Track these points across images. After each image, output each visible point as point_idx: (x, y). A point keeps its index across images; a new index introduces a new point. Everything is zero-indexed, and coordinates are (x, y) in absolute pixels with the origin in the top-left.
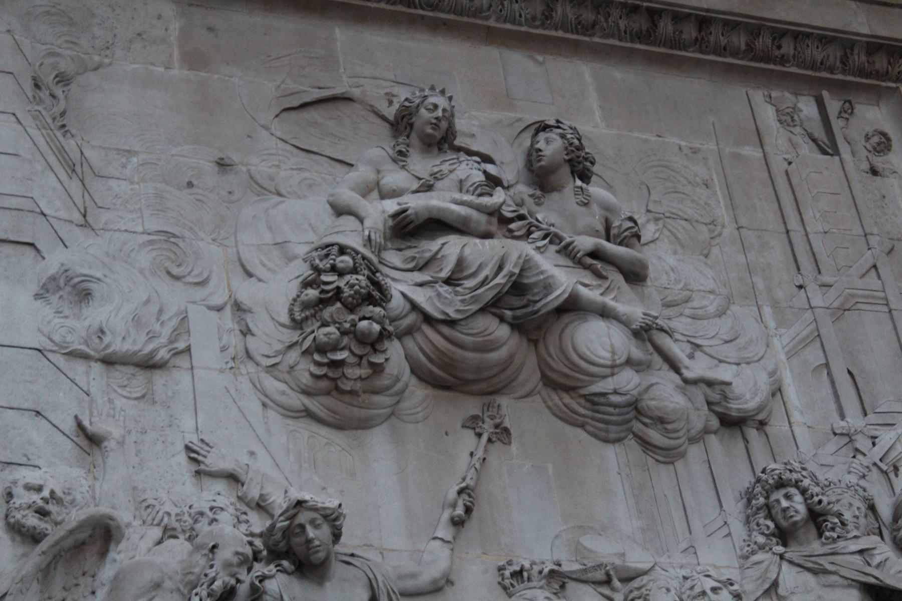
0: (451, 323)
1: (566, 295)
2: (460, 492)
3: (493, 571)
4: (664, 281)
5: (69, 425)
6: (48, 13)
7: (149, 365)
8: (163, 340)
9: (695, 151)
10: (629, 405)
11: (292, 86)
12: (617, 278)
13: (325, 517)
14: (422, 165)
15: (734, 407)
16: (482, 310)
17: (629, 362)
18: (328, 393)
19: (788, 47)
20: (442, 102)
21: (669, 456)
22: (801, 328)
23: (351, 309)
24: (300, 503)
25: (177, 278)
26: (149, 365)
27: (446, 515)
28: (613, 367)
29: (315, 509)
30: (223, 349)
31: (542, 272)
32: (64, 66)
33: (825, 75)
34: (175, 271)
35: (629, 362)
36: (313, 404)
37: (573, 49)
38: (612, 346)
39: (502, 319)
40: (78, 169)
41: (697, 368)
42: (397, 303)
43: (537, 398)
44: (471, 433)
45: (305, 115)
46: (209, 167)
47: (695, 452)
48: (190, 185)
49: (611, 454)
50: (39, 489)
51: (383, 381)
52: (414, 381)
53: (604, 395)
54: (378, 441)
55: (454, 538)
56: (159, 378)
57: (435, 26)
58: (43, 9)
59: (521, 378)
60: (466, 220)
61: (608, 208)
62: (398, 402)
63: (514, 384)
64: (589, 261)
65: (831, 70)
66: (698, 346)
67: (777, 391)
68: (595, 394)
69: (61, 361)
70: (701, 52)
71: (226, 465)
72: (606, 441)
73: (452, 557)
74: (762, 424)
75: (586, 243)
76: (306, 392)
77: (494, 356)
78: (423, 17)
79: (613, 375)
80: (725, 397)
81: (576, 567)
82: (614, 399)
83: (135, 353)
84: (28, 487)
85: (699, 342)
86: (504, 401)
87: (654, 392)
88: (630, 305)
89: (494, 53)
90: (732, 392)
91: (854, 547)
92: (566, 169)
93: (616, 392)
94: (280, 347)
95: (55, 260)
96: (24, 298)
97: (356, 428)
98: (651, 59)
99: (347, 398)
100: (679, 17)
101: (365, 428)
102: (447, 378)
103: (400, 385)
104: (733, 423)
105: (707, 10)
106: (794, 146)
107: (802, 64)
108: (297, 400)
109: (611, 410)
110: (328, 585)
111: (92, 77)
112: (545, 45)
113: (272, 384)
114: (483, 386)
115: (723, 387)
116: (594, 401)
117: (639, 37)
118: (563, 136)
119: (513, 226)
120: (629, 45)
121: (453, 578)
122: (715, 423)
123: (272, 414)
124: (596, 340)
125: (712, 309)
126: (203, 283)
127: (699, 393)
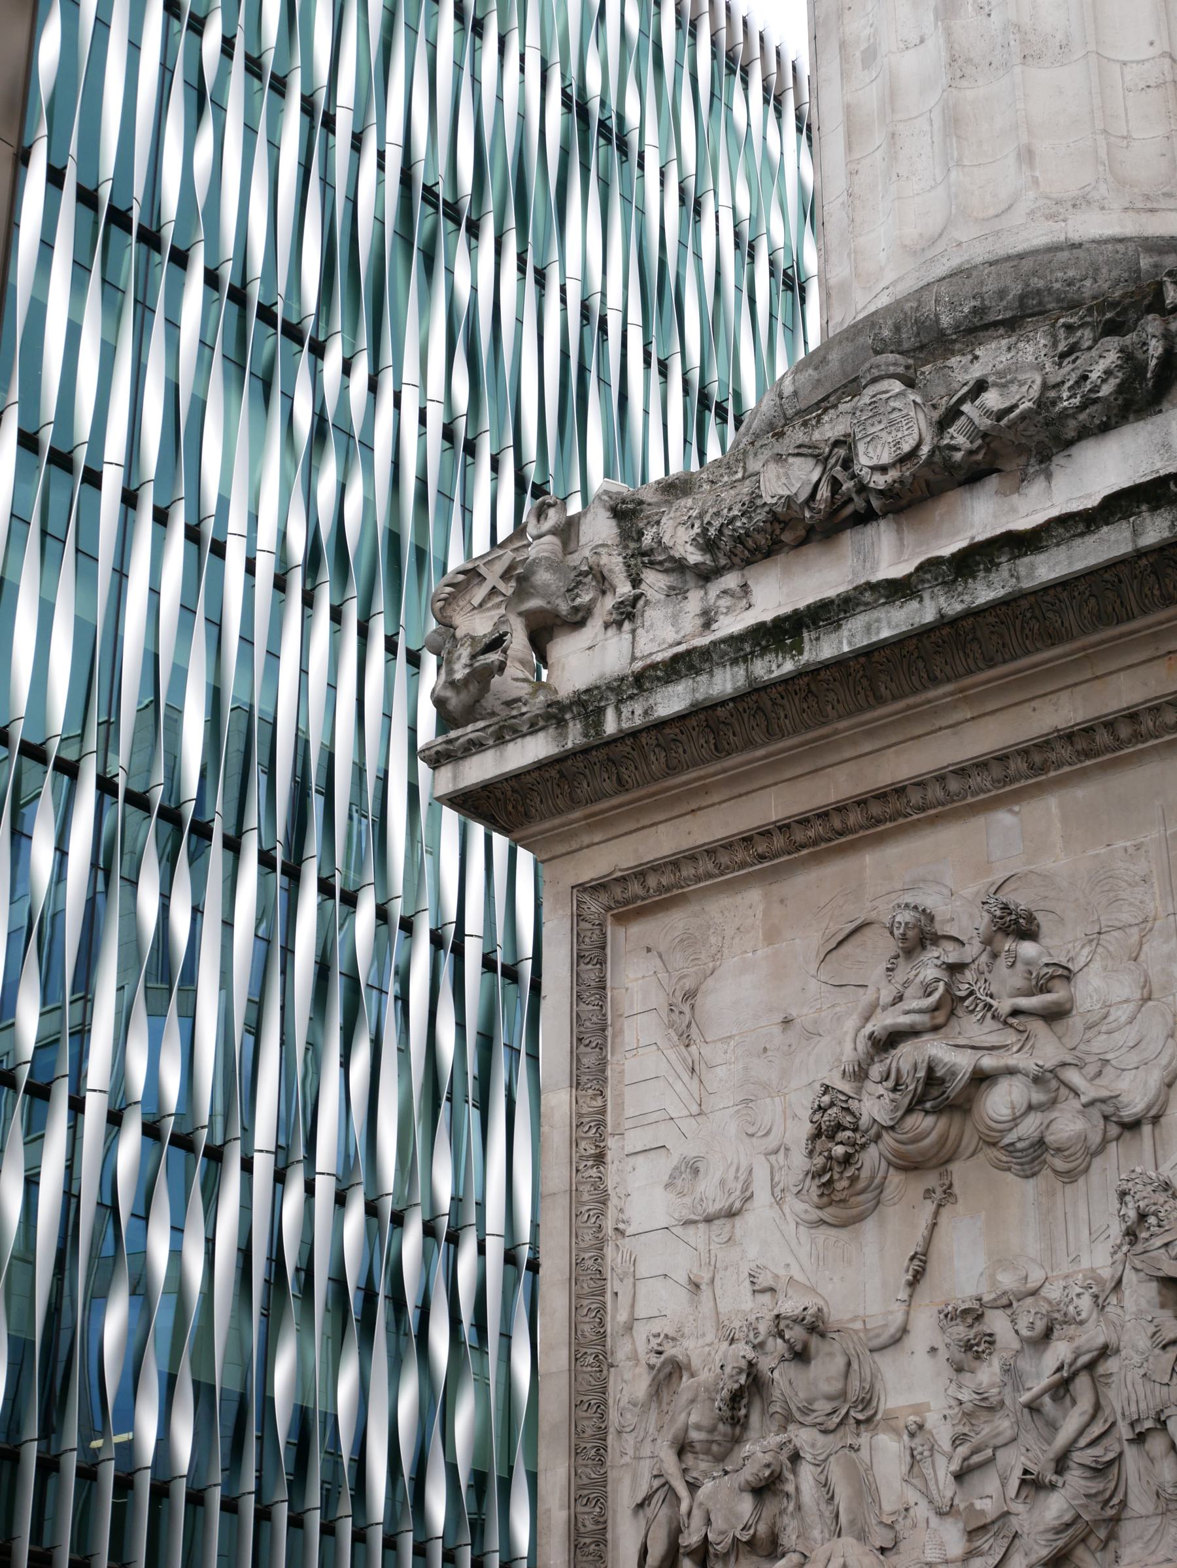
0: (892, 1128)
1: (967, 1075)
2: (912, 1258)
3: (936, 1314)
4: (1087, 1006)
5: (683, 1280)
6: (682, 941)
7: (731, 1214)
8: (738, 1193)
9: (1138, 847)
10: (1032, 1145)
11: (833, 928)
12: (1037, 1026)
13: (794, 1321)
14: (903, 972)
15: (1128, 1114)
16: (909, 1110)
17: (1030, 1108)
18: (830, 1204)
20: (906, 917)
21: (1069, 1177)
23: (831, 1137)
24: (778, 1316)
25: (753, 1135)
26: (731, 1214)
27: (903, 1281)
28: (1014, 1119)
29: (786, 1318)
30: (773, 1187)
31: (945, 1065)
32: (688, 984)
34: (751, 1131)
35: (1030, 1108)
36: (824, 1215)
37: (1040, 789)
38: (1012, 1102)
39: (927, 1112)
40: (697, 1068)
41: (1089, 1092)
42: (864, 1122)
43: (981, 1155)
44: (929, 1202)
45: (843, 950)
46: (777, 1030)
47: (1097, 1162)
48: (765, 1049)
49: (1030, 1185)
50: (659, 1335)
51: (861, 1185)
52: (892, 1170)
53: (1012, 1144)
54: (869, 1225)
55: (911, 1296)
56: (738, 1221)
57: (933, 821)
58: (678, 940)
59: (964, 1143)
60: (912, 1026)
61: (1028, 963)
62: (881, 1192)
63: (960, 1149)
64: (1011, 1020)
66: (1108, 1061)
68: (1008, 1145)
69: (678, 1230)
70: (1143, 742)
71: (765, 1284)
72: (1027, 1177)
73: (908, 1313)
74: (1155, 1120)
75: (1004, 1005)
76: (818, 1207)
77: (927, 1142)
78: (919, 820)
79: (1016, 1125)
80: (1118, 1109)
81: (993, 1296)
82: (1019, 1145)
83: (721, 1210)
84: (654, 1336)
85: (1108, 1057)
86: (956, 1168)
87: (1054, 1127)
88: (1046, 1049)
89: (978, 822)
90: (1121, 1102)
91: (1158, 1242)
92: (999, 936)
93: (1020, 1139)
94: (801, 1177)
95: (680, 1150)
96: (659, 1192)
97: (854, 1223)
98: (1104, 767)
99: (842, 1205)
100: (1109, 725)
101: (862, 1220)
102: (910, 1165)
103: (877, 1181)
104: (1132, 1126)
105: (1128, 708)
108: (815, 1214)
109: (1019, 1154)
110: (813, 1362)
111: (710, 982)
112: (1018, 796)
113: (800, 1207)
114: (934, 1162)
115: (1114, 1101)
116: (1010, 1148)
117: (1087, 754)
118: (989, 912)
119: (967, 1003)
120: (1079, 766)
121: (909, 1328)
122: (1114, 1130)
123: (801, 1228)
124: (1000, 1102)
125: (1123, 1019)
126: (767, 1134)
127: (1095, 1113)
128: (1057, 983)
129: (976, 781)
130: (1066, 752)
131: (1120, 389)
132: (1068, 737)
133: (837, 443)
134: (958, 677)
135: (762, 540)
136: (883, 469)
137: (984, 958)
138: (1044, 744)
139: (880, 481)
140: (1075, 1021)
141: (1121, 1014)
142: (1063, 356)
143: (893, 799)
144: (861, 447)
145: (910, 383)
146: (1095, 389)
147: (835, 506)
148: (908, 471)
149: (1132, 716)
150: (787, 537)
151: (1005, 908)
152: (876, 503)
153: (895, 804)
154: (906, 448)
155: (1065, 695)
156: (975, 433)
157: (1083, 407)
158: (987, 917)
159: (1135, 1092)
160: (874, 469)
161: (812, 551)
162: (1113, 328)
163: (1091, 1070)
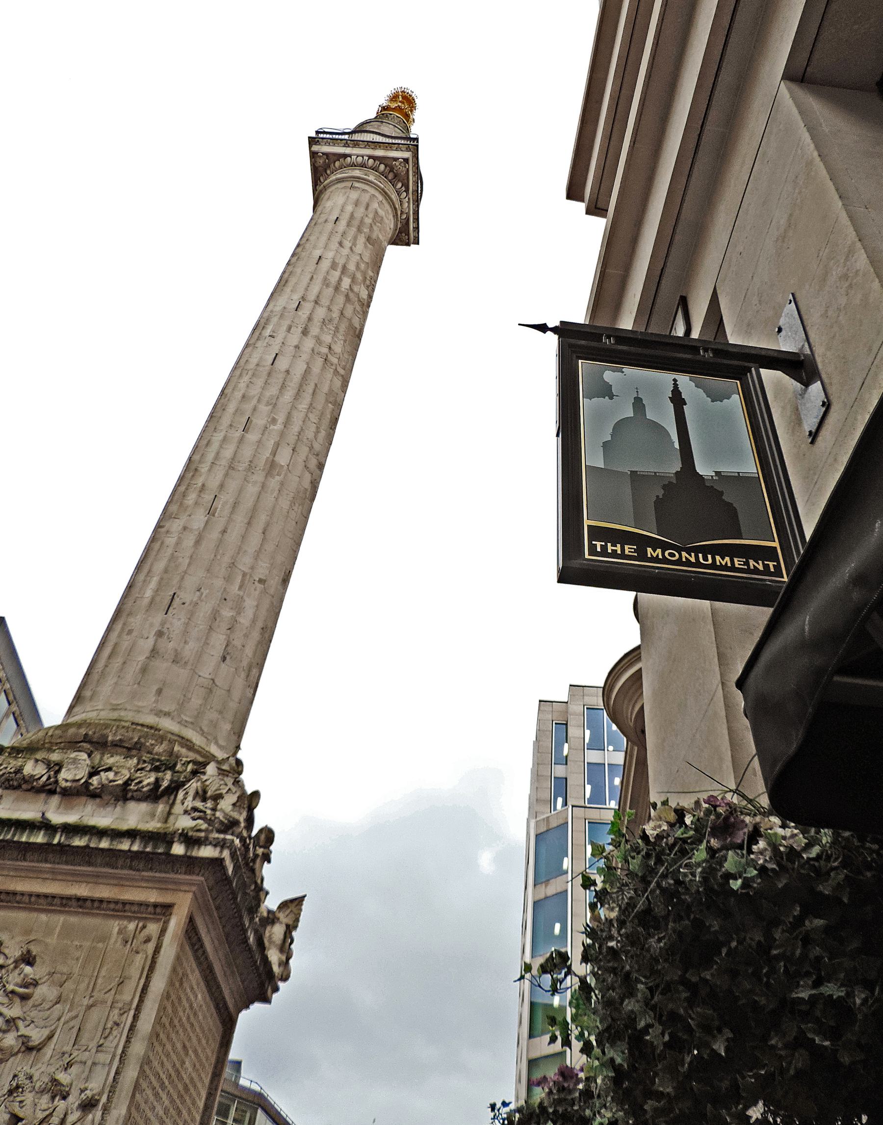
12: (17, 1000)
15: (30, 1044)
19: (127, 907)
22: (73, 1014)
33: (139, 915)
37: (60, 912)
41: (23, 1031)
61: (26, 976)
64: (10, 995)
65: (142, 913)
67: (50, 1037)
74: (39, 1050)
75: (10, 987)
98: (83, 913)
100: (93, 901)
104: (30, 1049)
106: (116, 942)
107: (131, 912)
117: (81, 907)
122: (23, 1049)
128: (32, 987)
129: (41, 901)
130: (74, 903)
131: (151, 790)
132: (78, 899)
133: (57, 764)
134: (54, 863)
135: (15, 783)
136: (67, 781)
137: (12, 966)
138: (69, 898)
139: (64, 784)
140: (30, 1002)
141: (46, 1006)
142: (139, 770)
143: (11, 895)
144: (63, 770)
145: (89, 756)
146: (143, 787)
147: (44, 786)
148: (74, 784)
149: (101, 901)
150: (24, 786)
151: (29, 952)
152: (58, 790)
153: (11, 897)
154: (77, 778)
155: (85, 884)
156: (100, 783)
157: (136, 791)
158: (20, 953)
159: (36, 1035)
160: (64, 779)
161: (30, 795)
162: (156, 769)
163: (27, 1023)
